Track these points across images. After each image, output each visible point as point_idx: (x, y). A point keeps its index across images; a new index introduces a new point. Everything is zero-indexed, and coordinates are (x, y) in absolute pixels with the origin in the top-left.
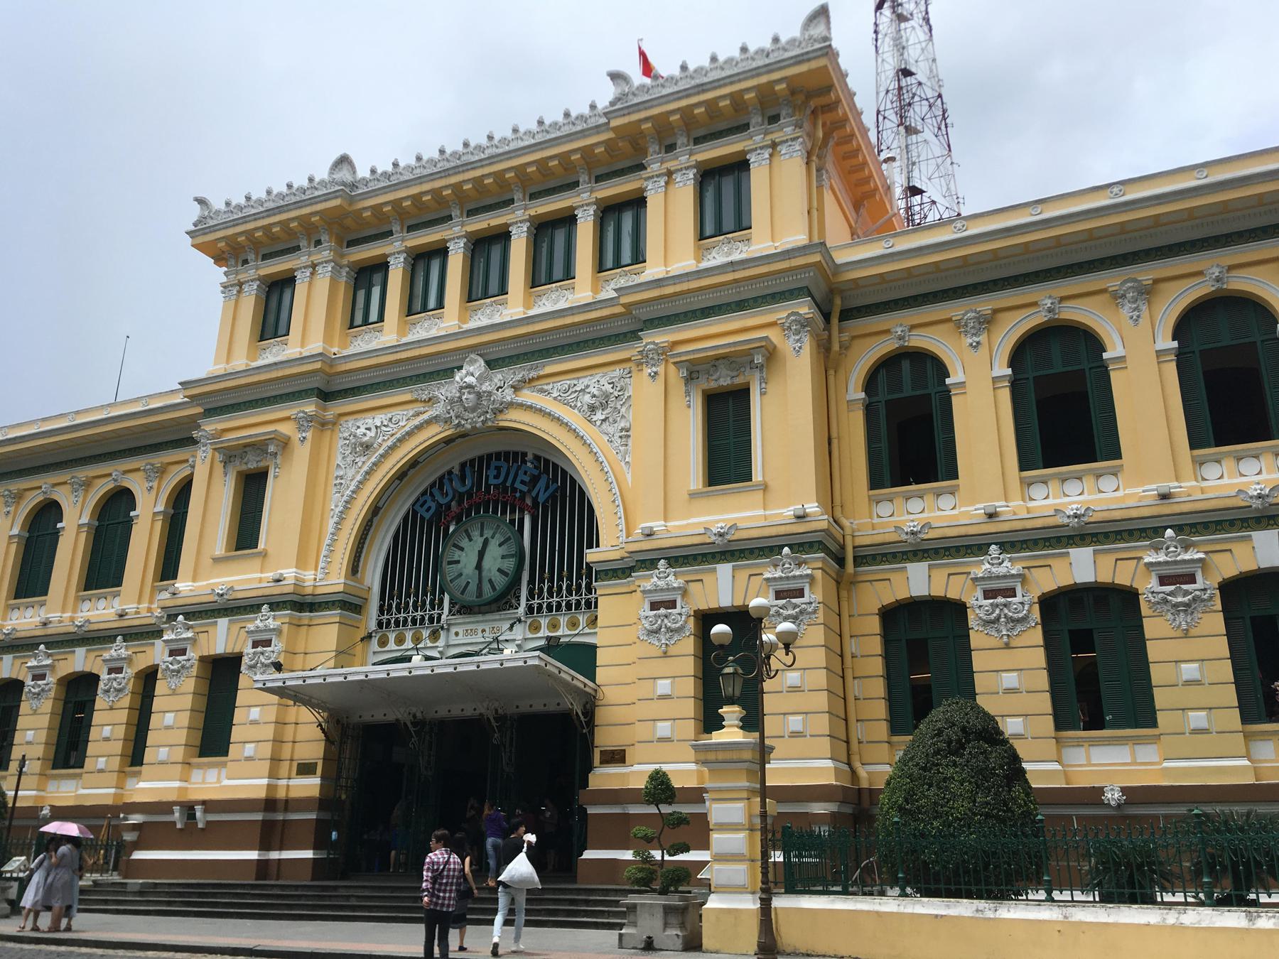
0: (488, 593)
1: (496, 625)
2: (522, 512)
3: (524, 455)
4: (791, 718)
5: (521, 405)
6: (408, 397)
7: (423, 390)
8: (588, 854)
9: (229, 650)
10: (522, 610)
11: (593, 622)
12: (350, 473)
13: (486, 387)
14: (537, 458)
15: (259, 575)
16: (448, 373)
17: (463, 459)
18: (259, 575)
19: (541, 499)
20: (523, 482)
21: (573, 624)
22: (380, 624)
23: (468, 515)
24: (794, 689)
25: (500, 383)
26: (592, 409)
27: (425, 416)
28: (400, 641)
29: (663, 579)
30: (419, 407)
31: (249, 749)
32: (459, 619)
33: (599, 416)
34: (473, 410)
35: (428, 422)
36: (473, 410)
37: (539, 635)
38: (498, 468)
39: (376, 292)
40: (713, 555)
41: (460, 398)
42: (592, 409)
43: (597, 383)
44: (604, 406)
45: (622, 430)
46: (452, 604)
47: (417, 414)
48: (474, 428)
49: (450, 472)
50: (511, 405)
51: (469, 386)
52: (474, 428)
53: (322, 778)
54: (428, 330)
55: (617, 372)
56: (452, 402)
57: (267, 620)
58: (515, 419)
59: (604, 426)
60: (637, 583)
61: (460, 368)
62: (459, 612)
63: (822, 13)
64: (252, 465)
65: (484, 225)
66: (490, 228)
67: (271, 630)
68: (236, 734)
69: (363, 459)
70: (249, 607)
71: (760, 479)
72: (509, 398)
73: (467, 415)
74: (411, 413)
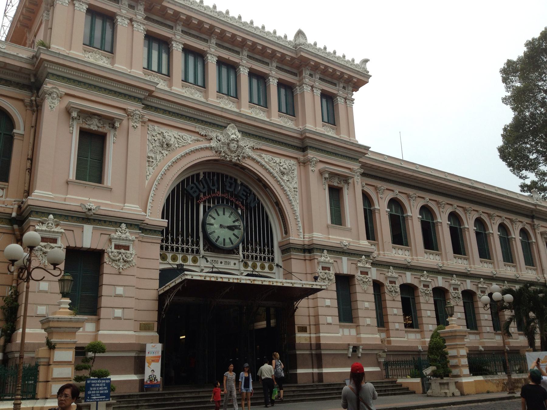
0: (228, 246)
1: (227, 260)
2: (237, 207)
3: (236, 180)
4: (116, 310)
5: (253, 159)
6: (193, 129)
7: (203, 130)
8: (299, 371)
9: (94, 247)
10: (242, 256)
11: (271, 268)
12: (159, 157)
13: (242, 143)
14: (242, 184)
15: (109, 202)
16: (222, 127)
17: (206, 171)
18: (109, 202)
19: (252, 205)
20: (243, 194)
21: (263, 267)
22: (162, 247)
23: (209, 202)
24: (367, 309)
25: (247, 144)
26: (283, 173)
27: (208, 145)
28: (174, 259)
29: (325, 258)
30: (201, 138)
31: (118, 313)
32: (208, 254)
33: (285, 178)
34: (232, 152)
35: (207, 148)
36: (232, 152)
37: (196, 265)
38: (231, 184)
39: (155, 54)
40: (340, 252)
41: (228, 144)
42: (283, 173)
43: (286, 163)
44: (288, 174)
45: (294, 188)
46: (204, 246)
47: (198, 140)
48: (231, 161)
49: (198, 175)
50: (249, 157)
51: (237, 141)
52: (231, 161)
53: (159, 332)
54: (226, 105)
55: (293, 162)
56: (223, 143)
57: (125, 234)
58: (248, 163)
59: (288, 183)
60: (316, 257)
61: (226, 127)
62: (207, 250)
63: (366, 61)
64: (94, 128)
65: (227, 57)
66: (228, 60)
67: (130, 240)
68: (104, 301)
69: (167, 152)
70: (114, 222)
71: (349, 226)
72: (250, 154)
73: (229, 153)
74: (196, 138)
